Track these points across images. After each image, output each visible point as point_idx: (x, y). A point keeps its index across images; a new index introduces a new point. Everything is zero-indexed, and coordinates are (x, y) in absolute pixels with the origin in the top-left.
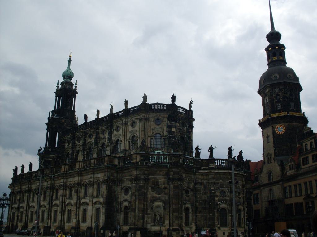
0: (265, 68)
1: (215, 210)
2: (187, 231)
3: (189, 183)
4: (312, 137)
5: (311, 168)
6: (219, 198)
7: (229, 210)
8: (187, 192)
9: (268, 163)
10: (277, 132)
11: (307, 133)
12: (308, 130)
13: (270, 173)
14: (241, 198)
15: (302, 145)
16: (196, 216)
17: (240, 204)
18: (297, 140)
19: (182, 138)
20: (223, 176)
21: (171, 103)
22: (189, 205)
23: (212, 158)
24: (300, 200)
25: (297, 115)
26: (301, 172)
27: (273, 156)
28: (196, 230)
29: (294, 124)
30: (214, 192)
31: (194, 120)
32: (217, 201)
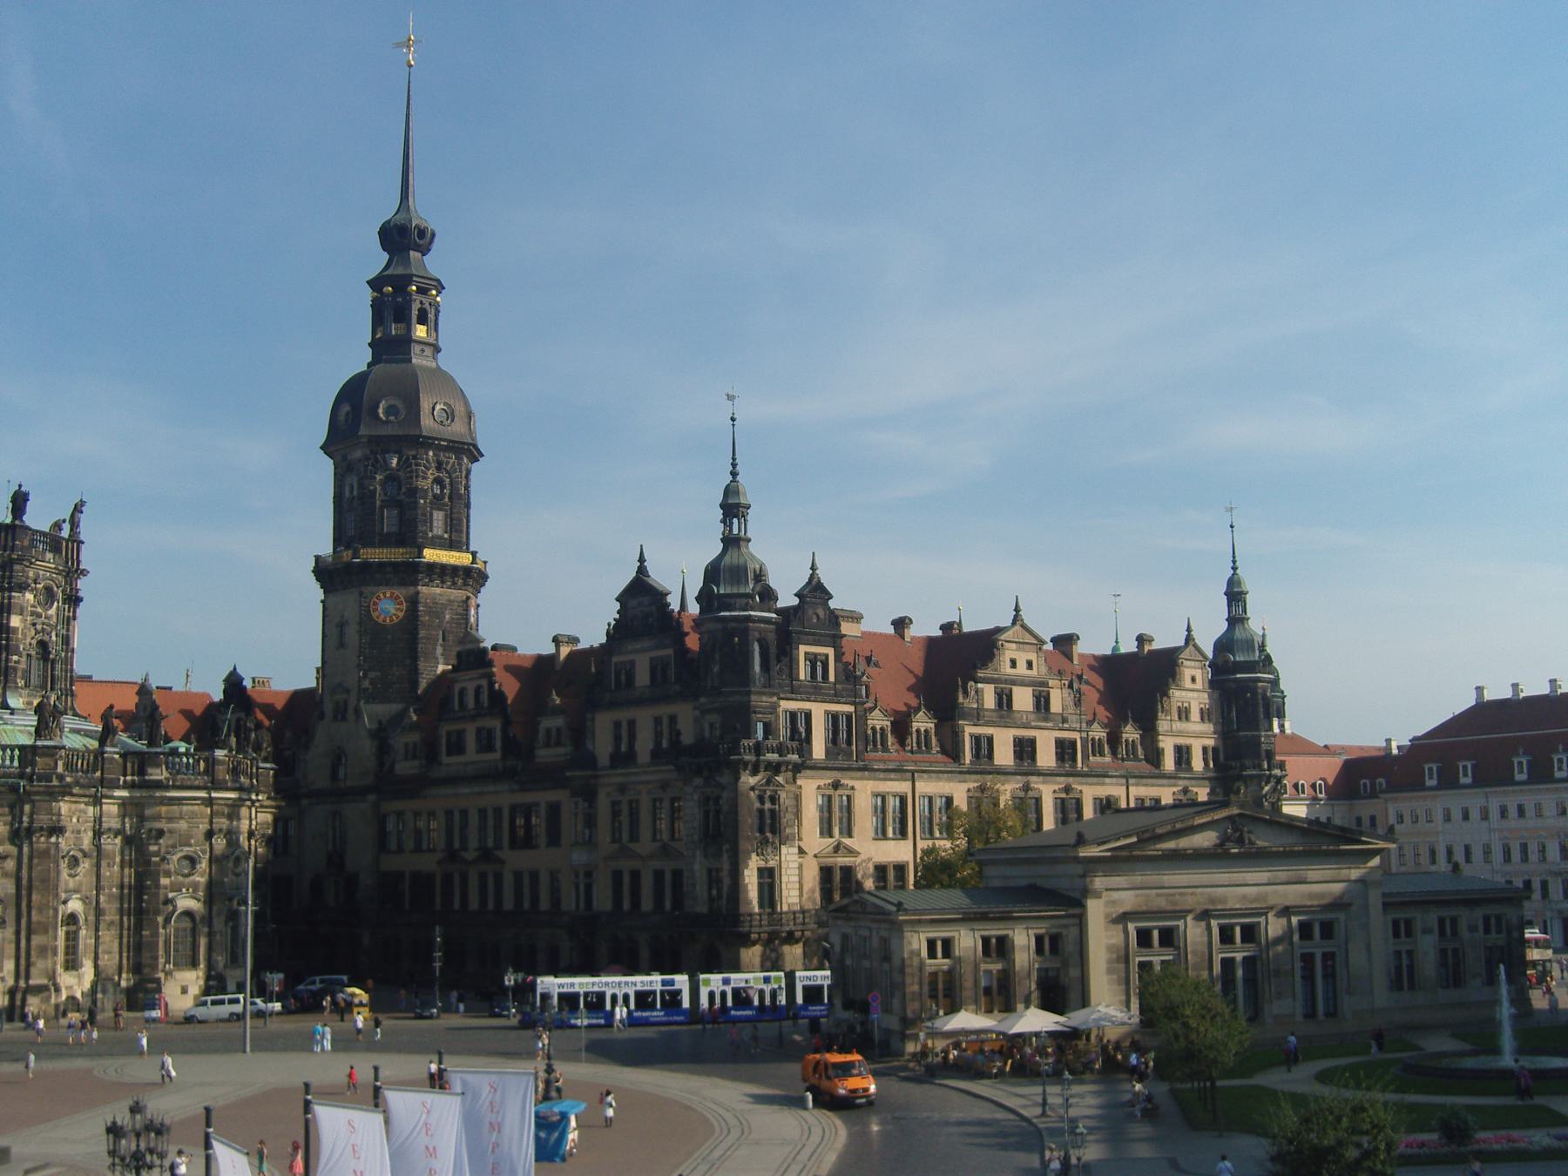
0: (358, 358)
2: (69, 988)
3: (79, 832)
8: (75, 862)
9: (335, 718)
13: (338, 757)
16: (97, 938)
18: (439, 650)
19: (43, 645)
21: (8, 521)
22: (75, 905)
24: (427, 863)
25: (452, 561)
28: (94, 985)
29: (438, 590)
31: (84, 573)
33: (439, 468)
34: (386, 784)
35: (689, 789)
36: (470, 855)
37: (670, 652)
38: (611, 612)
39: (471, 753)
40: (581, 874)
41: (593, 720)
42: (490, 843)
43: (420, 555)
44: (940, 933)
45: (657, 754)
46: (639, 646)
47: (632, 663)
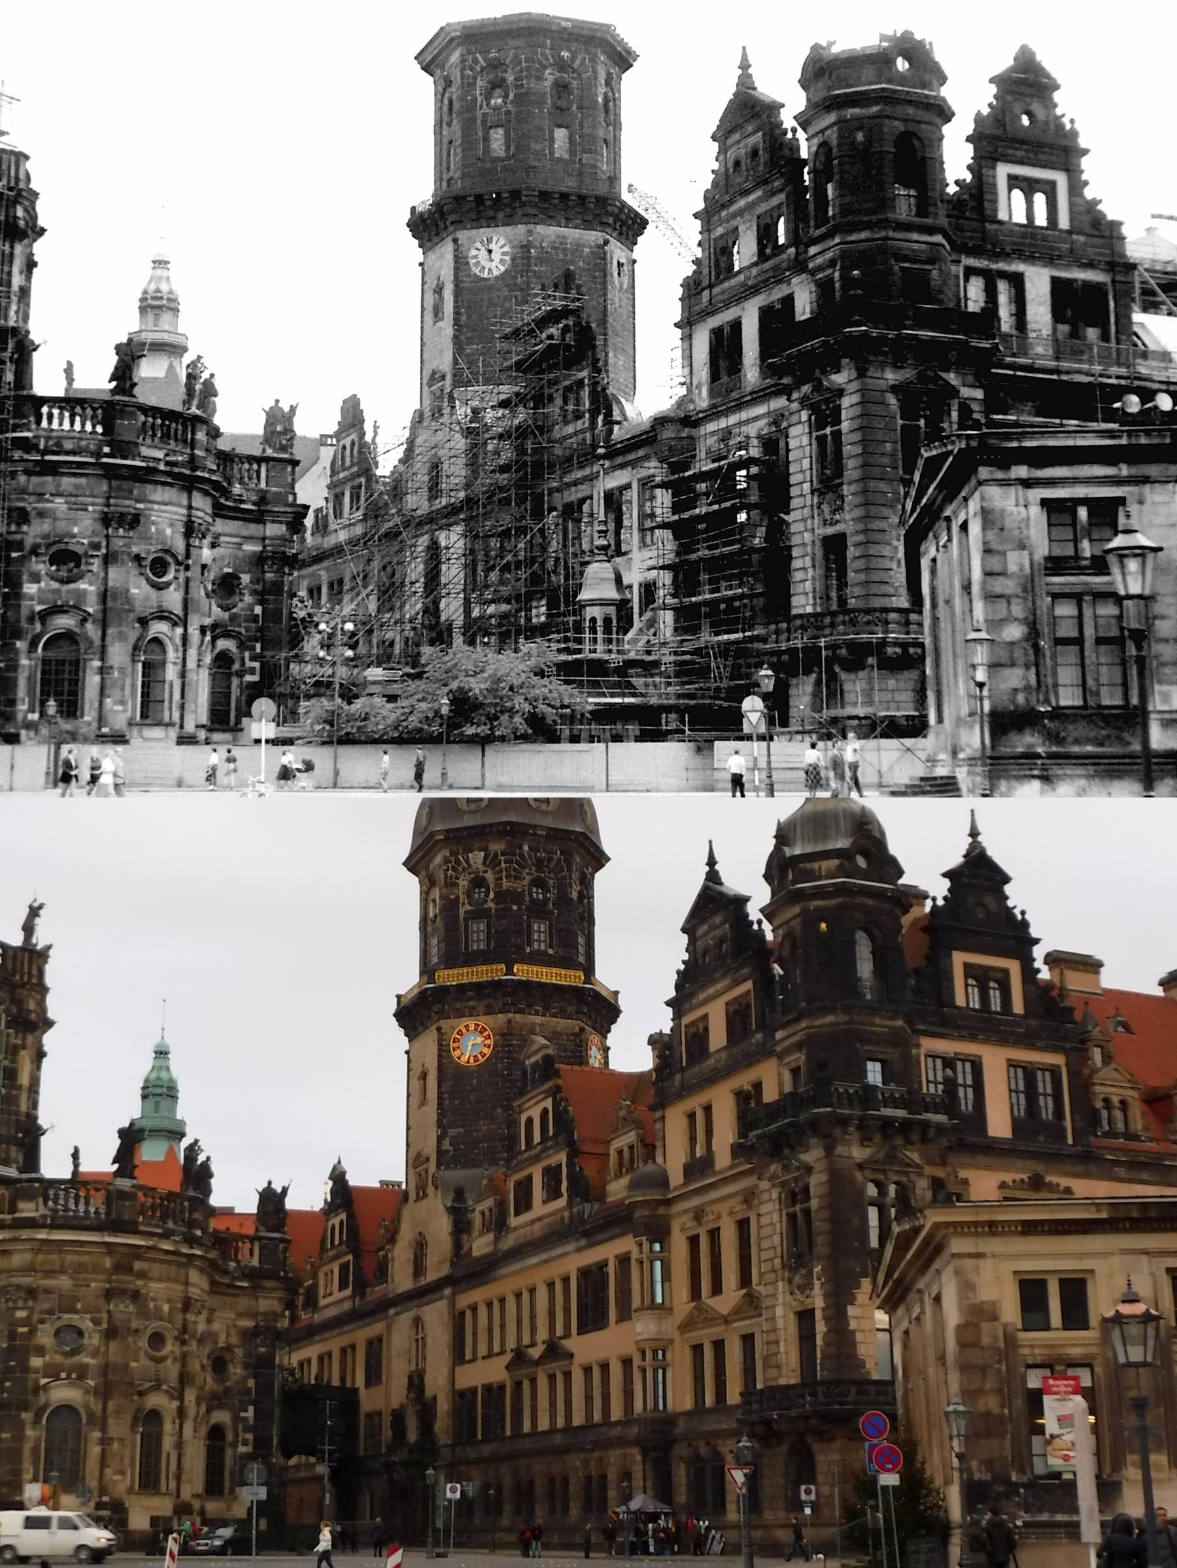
1: (24, 1415)
4: (547, 1086)
5: (537, 1226)
6: (47, 1358)
7: (91, 1415)
10: (458, 1053)
11: (535, 1065)
12: (538, 1057)
13: (420, 1246)
14: (164, 1359)
15: (516, 1123)
17: (157, 1388)
20: (77, 1258)
23: (33, 1175)
24: (494, 1371)
26: (509, 1242)
27: (432, 1166)
29: (538, 1019)
30: (26, 1329)
32: (37, 1371)
33: (540, 865)
34: (469, 1272)
35: (765, 1185)
36: (536, 1353)
37: (748, 985)
38: (674, 953)
39: (540, 1208)
40: (649, 1355)
41: (663, 1118)
42: (559, 1331)
43: (510, 971)
44: (1052, 1257)
45: (738, 1151)
46: (711, 991)
47: (705, 1017)
